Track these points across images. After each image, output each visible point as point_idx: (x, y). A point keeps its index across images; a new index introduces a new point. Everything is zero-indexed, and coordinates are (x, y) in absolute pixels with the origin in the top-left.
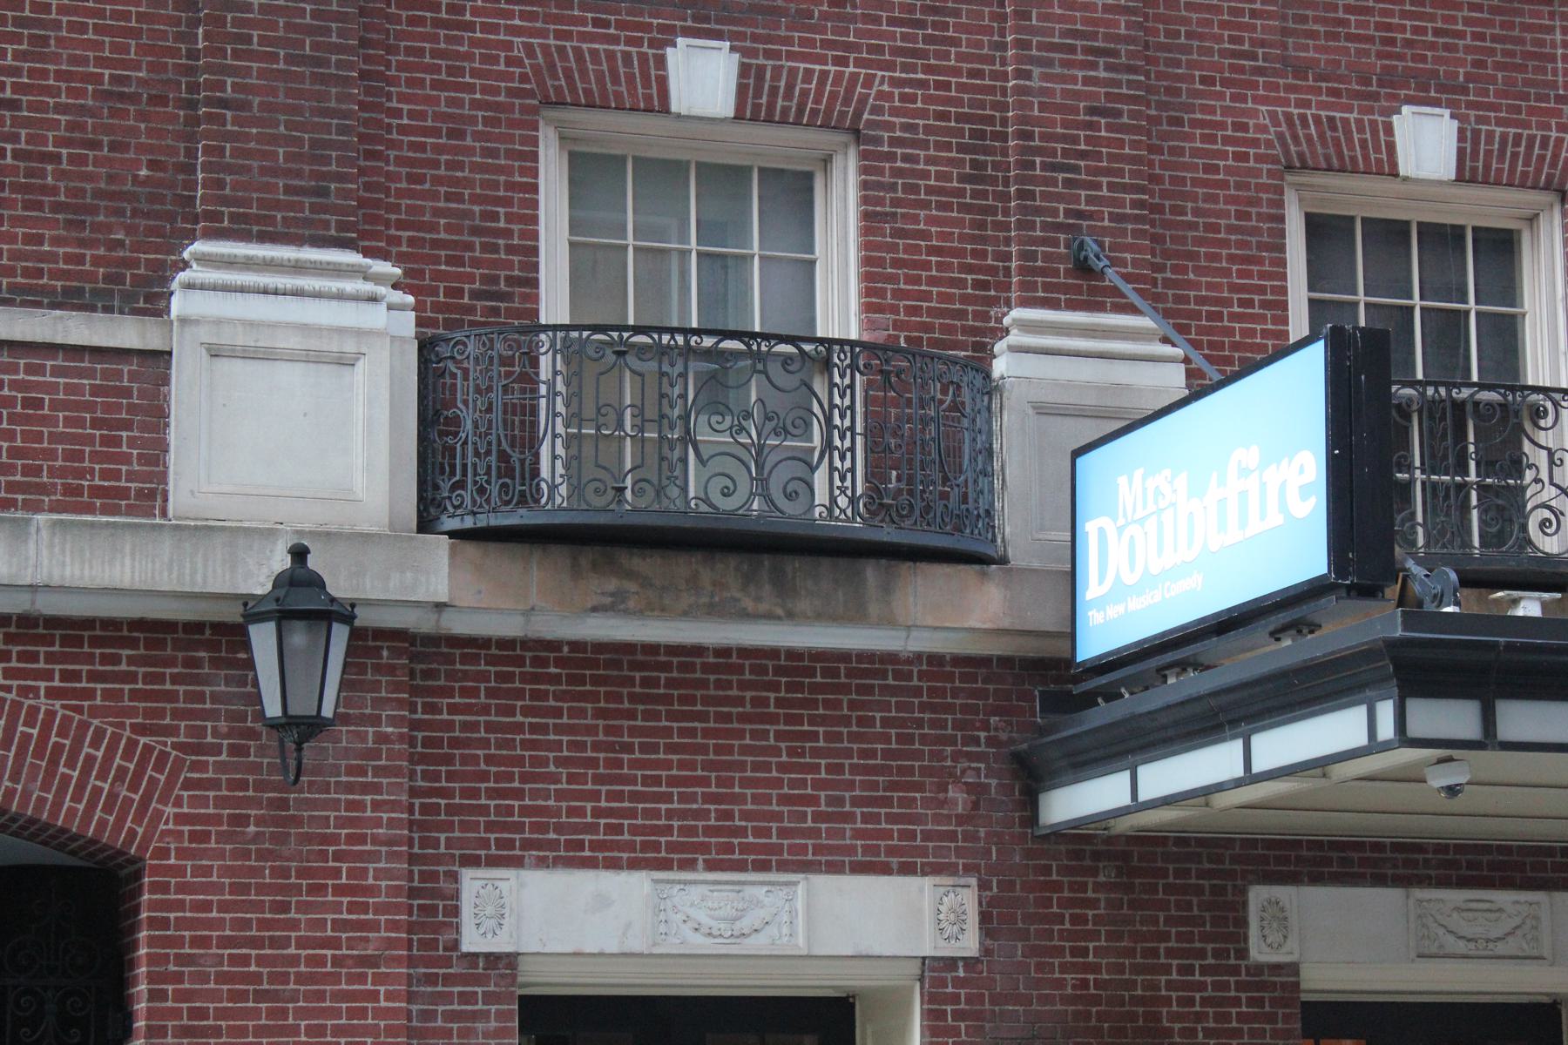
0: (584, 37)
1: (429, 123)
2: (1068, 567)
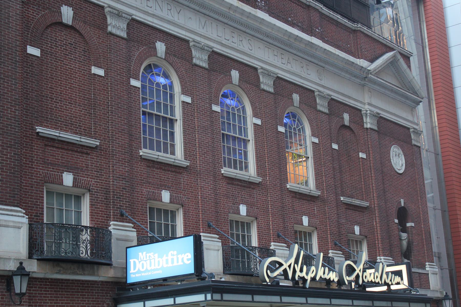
0: (51, 171)
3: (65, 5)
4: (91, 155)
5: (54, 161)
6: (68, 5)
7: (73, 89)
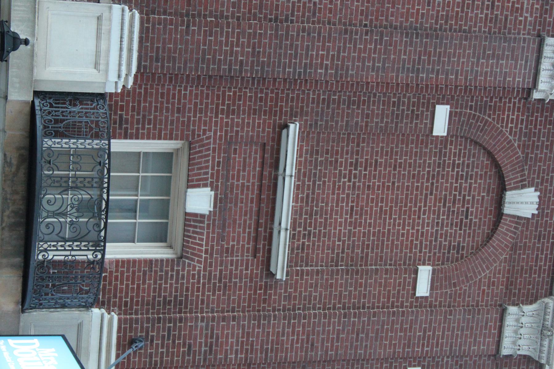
0: (214, 158)
1: (182, 101)
2: (20, 334)
3: (540, 197)
4: (253, 260)
5: (234, 167)
6: (540, 202)
7: (380, 218)
